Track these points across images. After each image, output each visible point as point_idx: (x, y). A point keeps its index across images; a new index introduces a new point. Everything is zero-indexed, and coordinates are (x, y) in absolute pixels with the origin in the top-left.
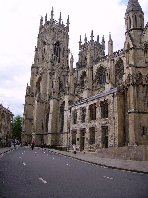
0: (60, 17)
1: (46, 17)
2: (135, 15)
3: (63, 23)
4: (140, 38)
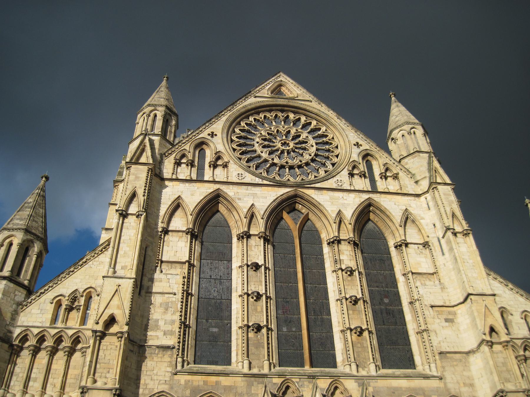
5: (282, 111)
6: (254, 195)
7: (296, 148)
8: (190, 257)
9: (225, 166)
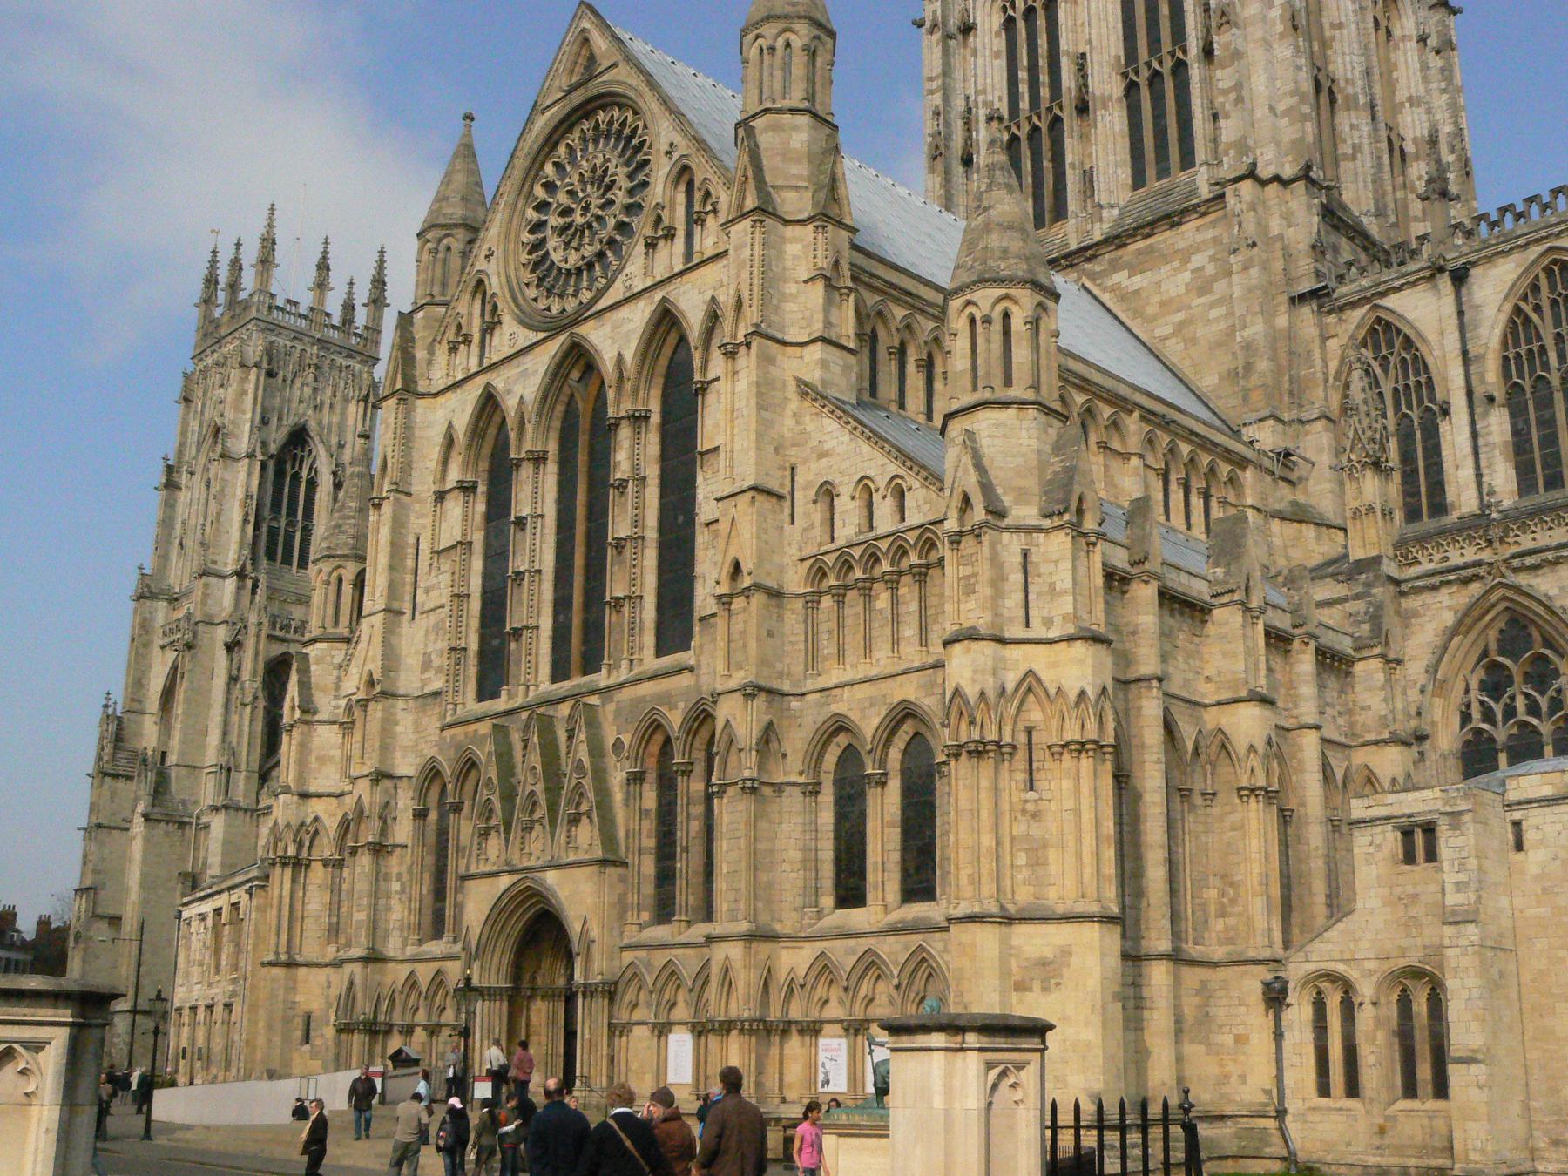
0: (323, 266)
1: (236, 265)
2: (335, 574)
3: (350, 294)
4: (339, 678)
5: (587, 116)
6: (525, 374)
7: (602, 207)
8: (464, 534)
9: (500, 322)
